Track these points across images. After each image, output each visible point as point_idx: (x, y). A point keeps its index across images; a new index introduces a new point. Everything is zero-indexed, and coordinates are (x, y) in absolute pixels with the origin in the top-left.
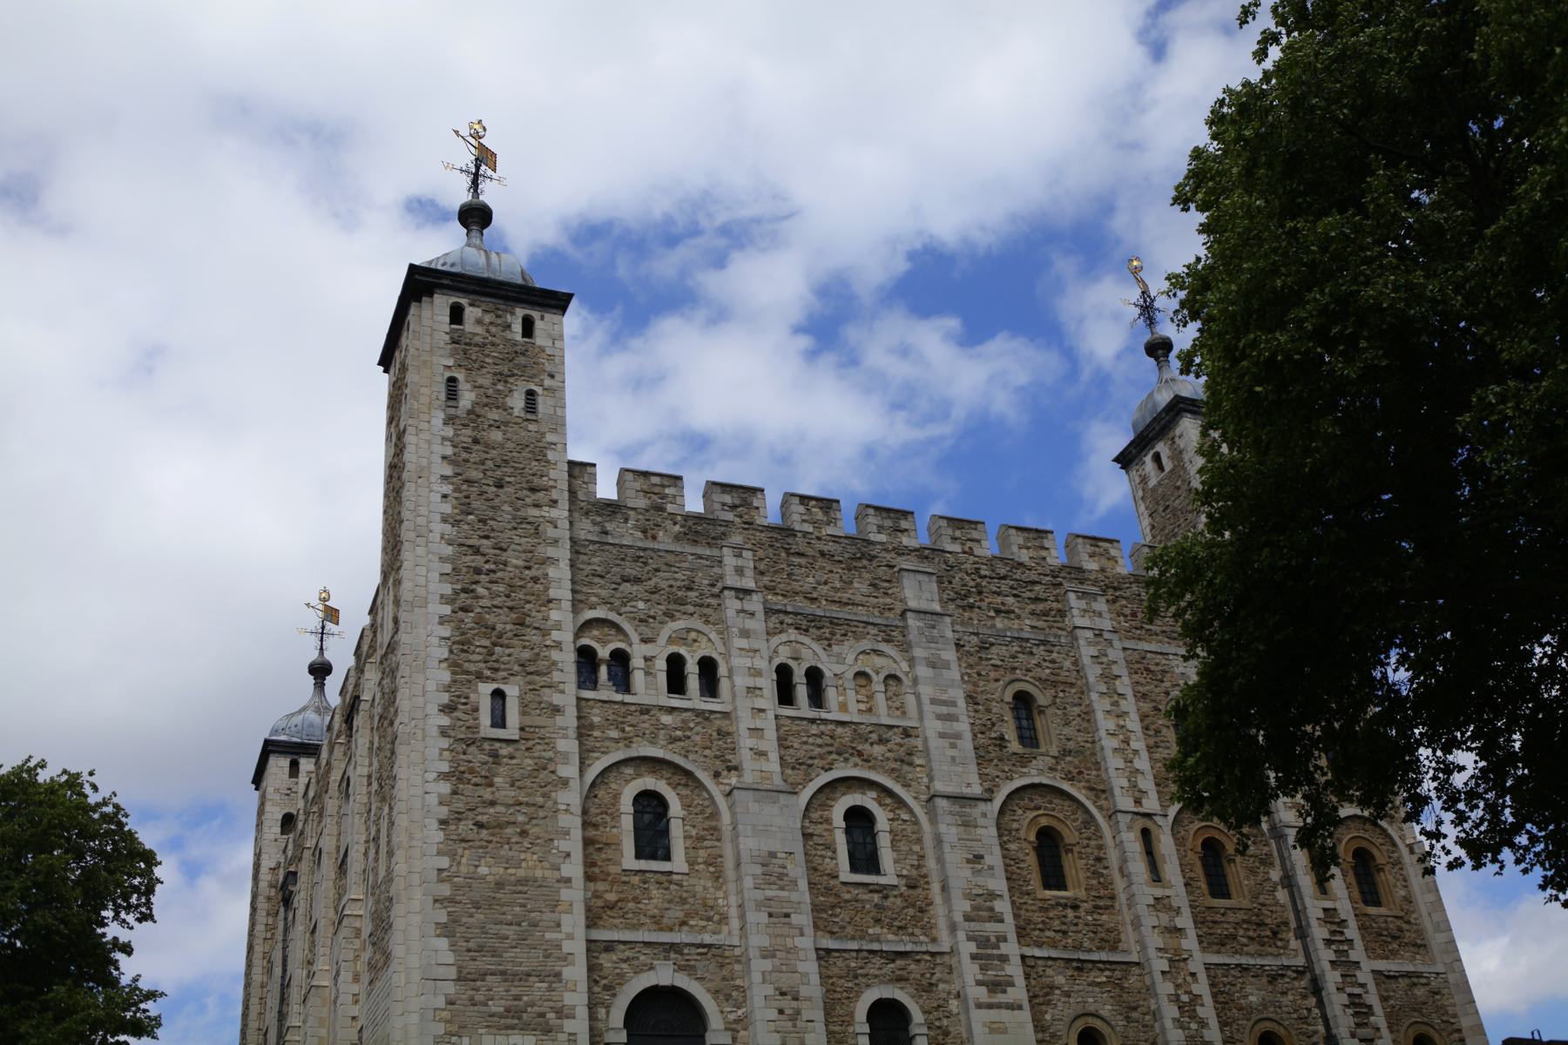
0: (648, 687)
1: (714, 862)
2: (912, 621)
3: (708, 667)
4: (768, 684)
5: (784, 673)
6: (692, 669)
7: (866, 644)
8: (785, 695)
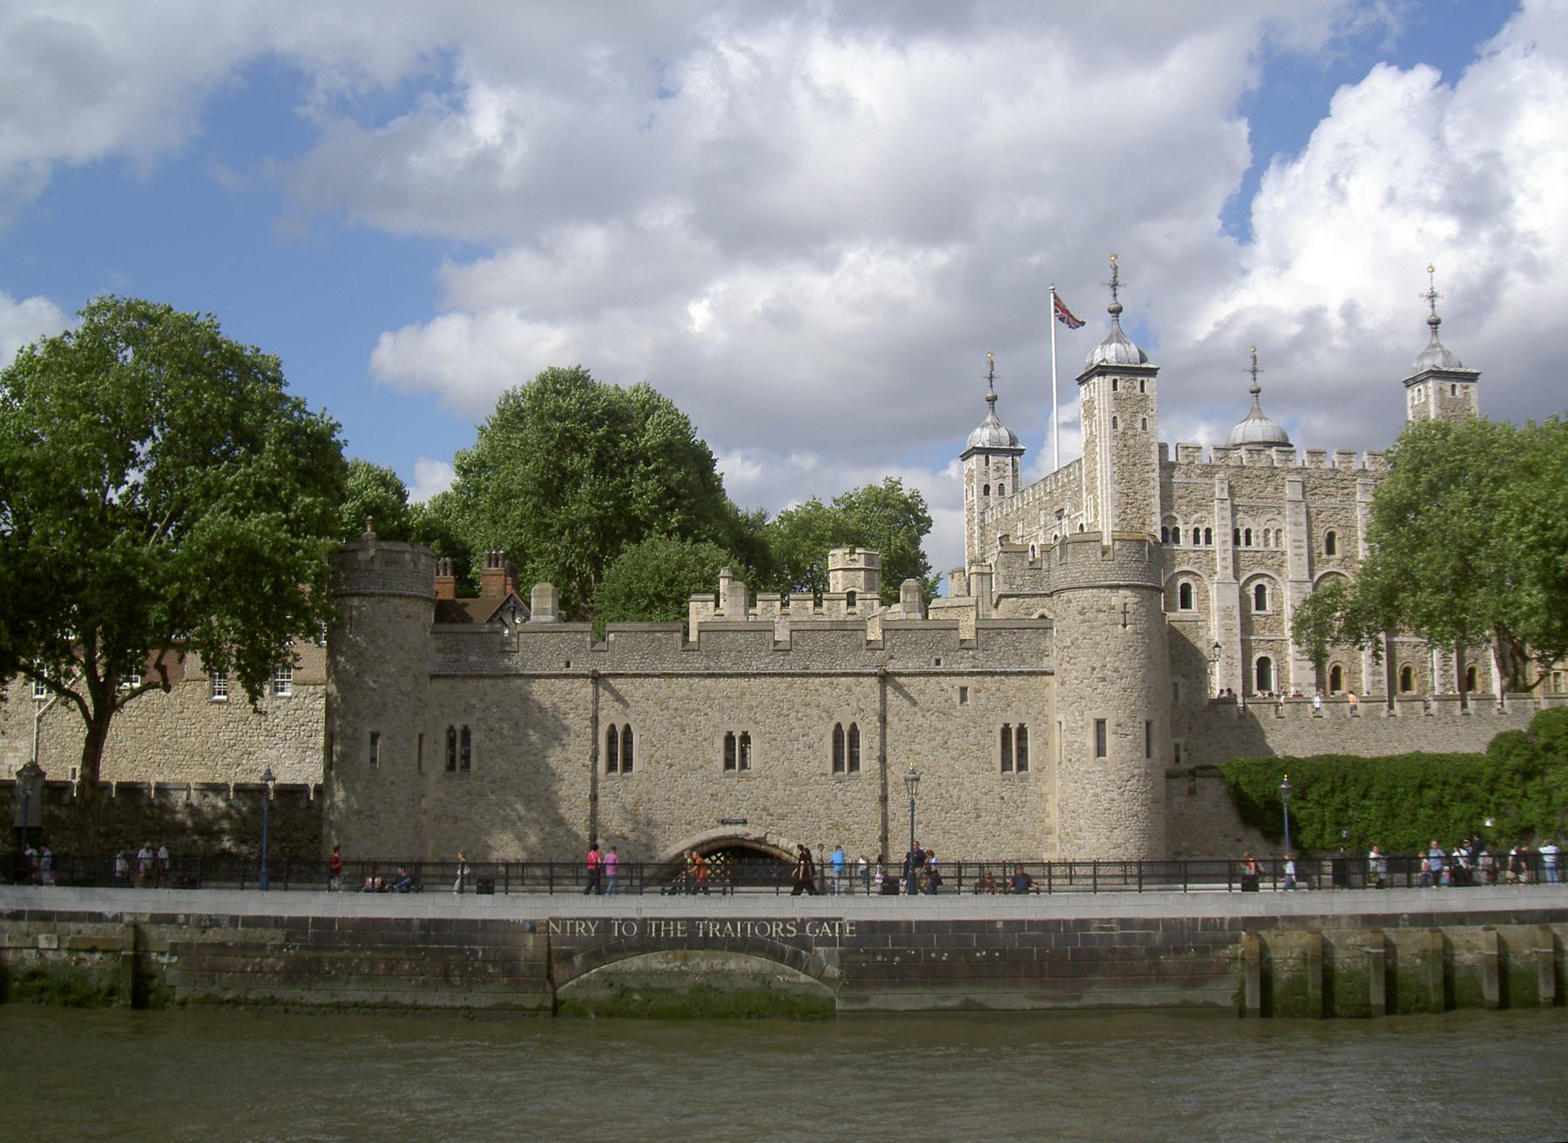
0: (1185, 542)
1: (1207, 608)
2: (1288, 506)
3: (1208, 531)
4: (1230, 539)
5: (1236, 532)
6: (1202, 534)
7: (1269, 516)
8: (1236, 541)
